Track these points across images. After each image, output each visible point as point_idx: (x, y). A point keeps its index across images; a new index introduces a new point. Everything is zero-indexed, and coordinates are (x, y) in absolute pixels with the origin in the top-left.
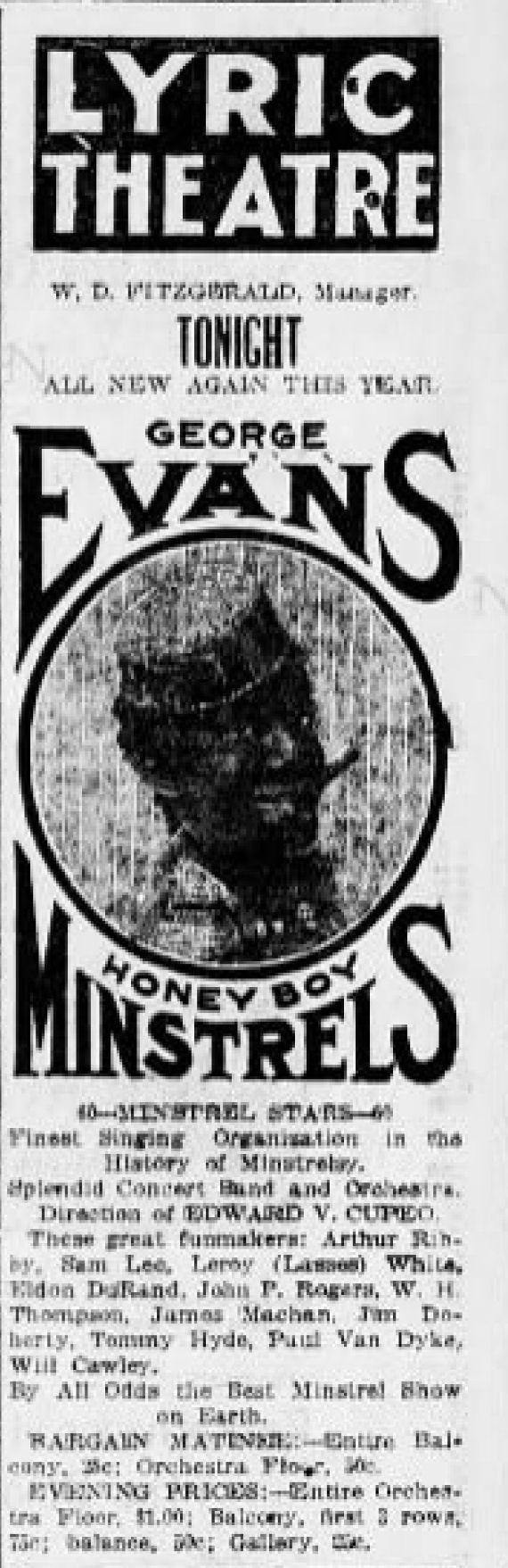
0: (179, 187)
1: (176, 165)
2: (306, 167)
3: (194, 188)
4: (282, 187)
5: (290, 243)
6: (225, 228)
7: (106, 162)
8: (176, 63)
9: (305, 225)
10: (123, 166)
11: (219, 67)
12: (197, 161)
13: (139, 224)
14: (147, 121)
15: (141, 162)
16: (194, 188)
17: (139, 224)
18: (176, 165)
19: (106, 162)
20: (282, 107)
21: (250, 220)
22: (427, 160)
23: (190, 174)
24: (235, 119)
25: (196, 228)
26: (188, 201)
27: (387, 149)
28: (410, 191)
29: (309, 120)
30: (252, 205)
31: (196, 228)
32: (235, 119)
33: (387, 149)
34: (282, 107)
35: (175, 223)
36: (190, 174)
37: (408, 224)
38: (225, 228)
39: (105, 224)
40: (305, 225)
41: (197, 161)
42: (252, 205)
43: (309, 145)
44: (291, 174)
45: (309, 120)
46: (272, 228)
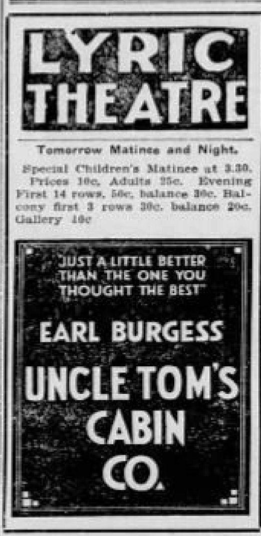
0: (102, 100)
2: (174, 89)
4: (162, 101)
5: (166, 125)
6: (130, 119)
8: (101, 38)
9: (174, 118)
11: (125, 40)
13: (81, 117)
14: (85, 67)
17: (81, 117)
19: (63, 88)
20: (161, 59)
21: (143, 115)
22: (243, 83)
24: (135, 64)
25: (113, 120)
26: (109, 106)
27: (221, 79)
28: (233, 99)
29: (176, 64)
30: (145, 108)
31: (113, 120)
32: (135, 64)
33: (221, 79)
34: (161, 59)
35: (101, 117)
37: (232, 116)
38: (130, 119)
40: (174, 118)
43: (174, 77)
44: (166, 93)
45: (176, 64)
46: (156, 119)
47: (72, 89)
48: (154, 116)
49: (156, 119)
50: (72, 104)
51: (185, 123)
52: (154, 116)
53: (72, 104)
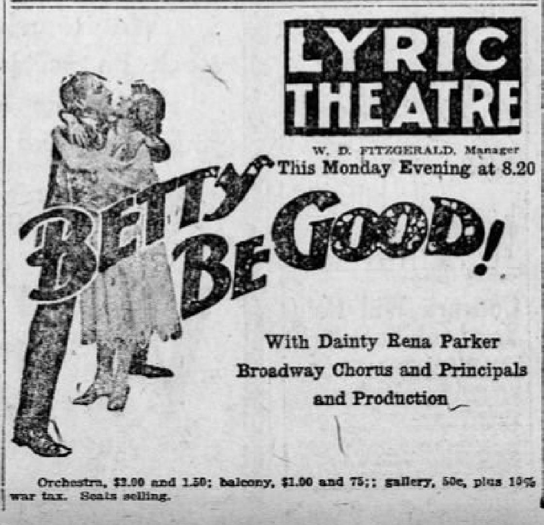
1: (366, 89)
3: (377, 101)
5: (435, 130)
6: (396, 123)
7: (325, 88)
9: (444, 121)
10: (335, 90)
12: (378, 86)
13: (344, 121)
15: (346, 88)
16: (377, 101)
17: (344, 121)
18: (366, 89)
21: (411, 118)
23: (374, 93)
25: (378, 123)
30: (413, 110)
31: (378, 123)
35: (366, 121)
36: (374, 93)
38: (396, 123)
39: (324, 122)
41: (378, 86)
42: (413, 110)
46: (425, 122)
47: (335, 90)
48: (422, 119)
49: (425, 122)
50: (335, 108)
51: (455, 128)
52: (422, 119)
53: (335, 108)
